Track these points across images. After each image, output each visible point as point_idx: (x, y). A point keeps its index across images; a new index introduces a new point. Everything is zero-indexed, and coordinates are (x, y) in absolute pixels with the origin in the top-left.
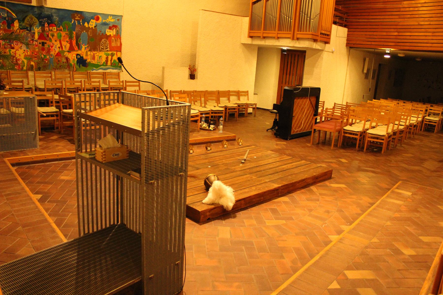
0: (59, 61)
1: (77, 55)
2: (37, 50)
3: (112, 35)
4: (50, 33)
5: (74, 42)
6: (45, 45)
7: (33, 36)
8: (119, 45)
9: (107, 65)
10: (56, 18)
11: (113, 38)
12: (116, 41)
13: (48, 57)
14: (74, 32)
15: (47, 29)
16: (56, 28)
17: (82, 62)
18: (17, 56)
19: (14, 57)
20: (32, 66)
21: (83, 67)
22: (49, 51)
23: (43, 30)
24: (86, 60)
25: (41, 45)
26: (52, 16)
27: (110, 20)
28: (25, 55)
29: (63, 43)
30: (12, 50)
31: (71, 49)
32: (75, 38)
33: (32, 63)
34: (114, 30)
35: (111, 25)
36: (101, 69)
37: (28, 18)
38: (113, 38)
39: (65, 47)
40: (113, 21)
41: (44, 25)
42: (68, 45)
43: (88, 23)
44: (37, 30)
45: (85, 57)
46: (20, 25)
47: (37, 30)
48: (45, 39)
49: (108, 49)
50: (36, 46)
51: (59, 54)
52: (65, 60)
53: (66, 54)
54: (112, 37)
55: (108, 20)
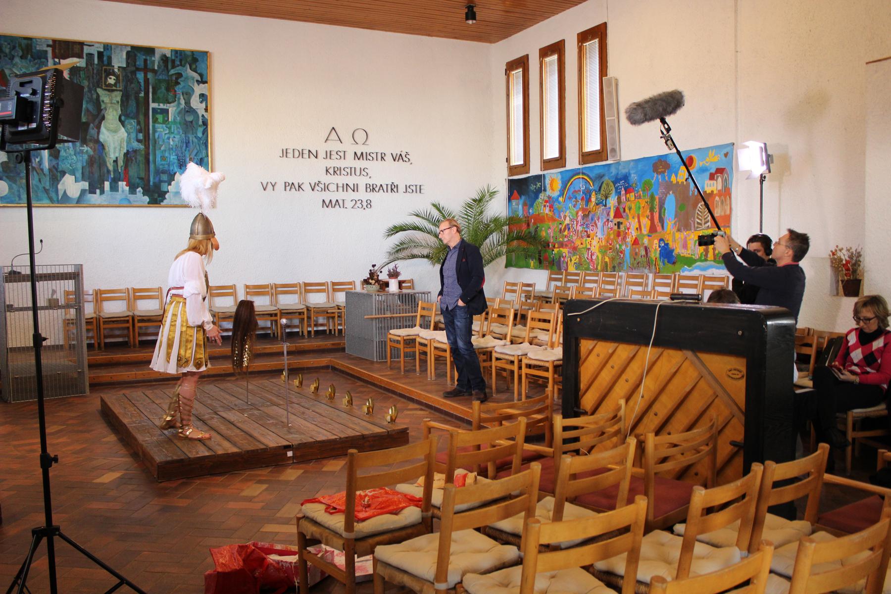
0: (636, 254)
1: (661, 240)
2: (612, 236)
3: (715, 192)
4: (628, 204)
5: (656, 216)
6: (621, 226)
7: (608, 215)
8: (728, 212)
9: (706, 260)
10: (634, 177)
11: (717, 198)
12: (722, 203)
13: (623, 247)
14: (657, 197)
15: (623, 198)
16: (632, 194)
17: (667, 254)
18: (592, 248)
19: (589, 249)
20: (606, 263)
21: (670, 265)
22: (624, 238)
23: (619, 202)
24: (672, 251)
25: (616, 227)
26: (630, 174)
27: (714, 161)
28: (600, 247)
29: (642, 219)
30: (589, 239)
31: (653, 229)
32: (657, 207)
33: (607, 259)
34: (720, 179)
35: (713, 171)
36: (696, 268)
37: (604, 185)
38: (717, 198)
39: (645, 226)
40: (716, 159)
41: (620, 193)
42: (649, 222)
43: (676, 176)
44: (612, 201)
45: (671, 245)
46: (597, 199)
47: (612, 201)
48: (621, 217)
49: (709, 224)
50: (611, 229)
51: (636, 242)
52: (643, 253)
53: (646, 241)
54: (716, 195)
55: (708, 159)
